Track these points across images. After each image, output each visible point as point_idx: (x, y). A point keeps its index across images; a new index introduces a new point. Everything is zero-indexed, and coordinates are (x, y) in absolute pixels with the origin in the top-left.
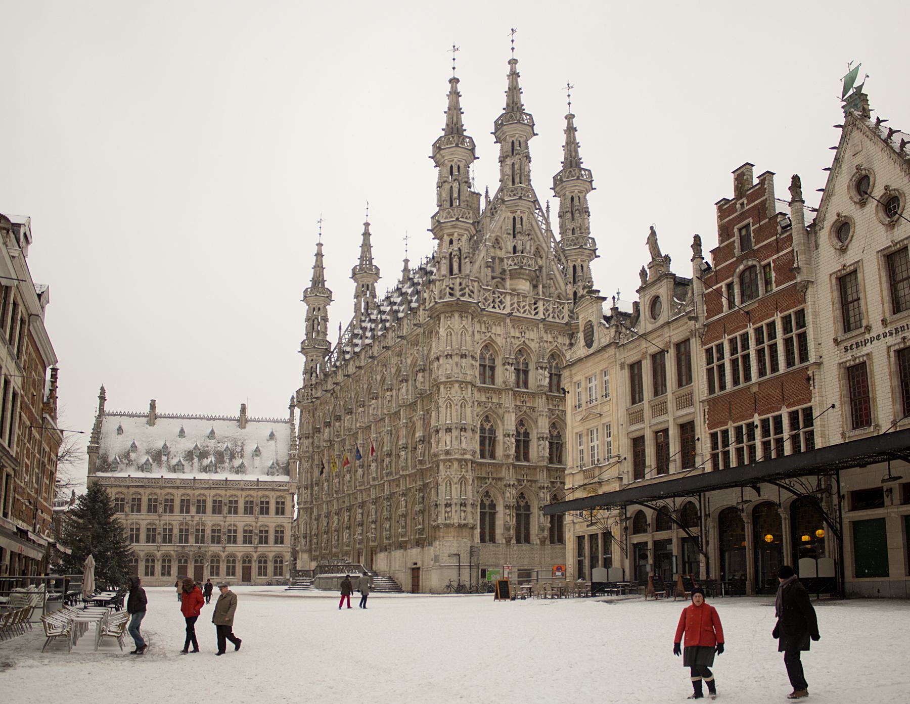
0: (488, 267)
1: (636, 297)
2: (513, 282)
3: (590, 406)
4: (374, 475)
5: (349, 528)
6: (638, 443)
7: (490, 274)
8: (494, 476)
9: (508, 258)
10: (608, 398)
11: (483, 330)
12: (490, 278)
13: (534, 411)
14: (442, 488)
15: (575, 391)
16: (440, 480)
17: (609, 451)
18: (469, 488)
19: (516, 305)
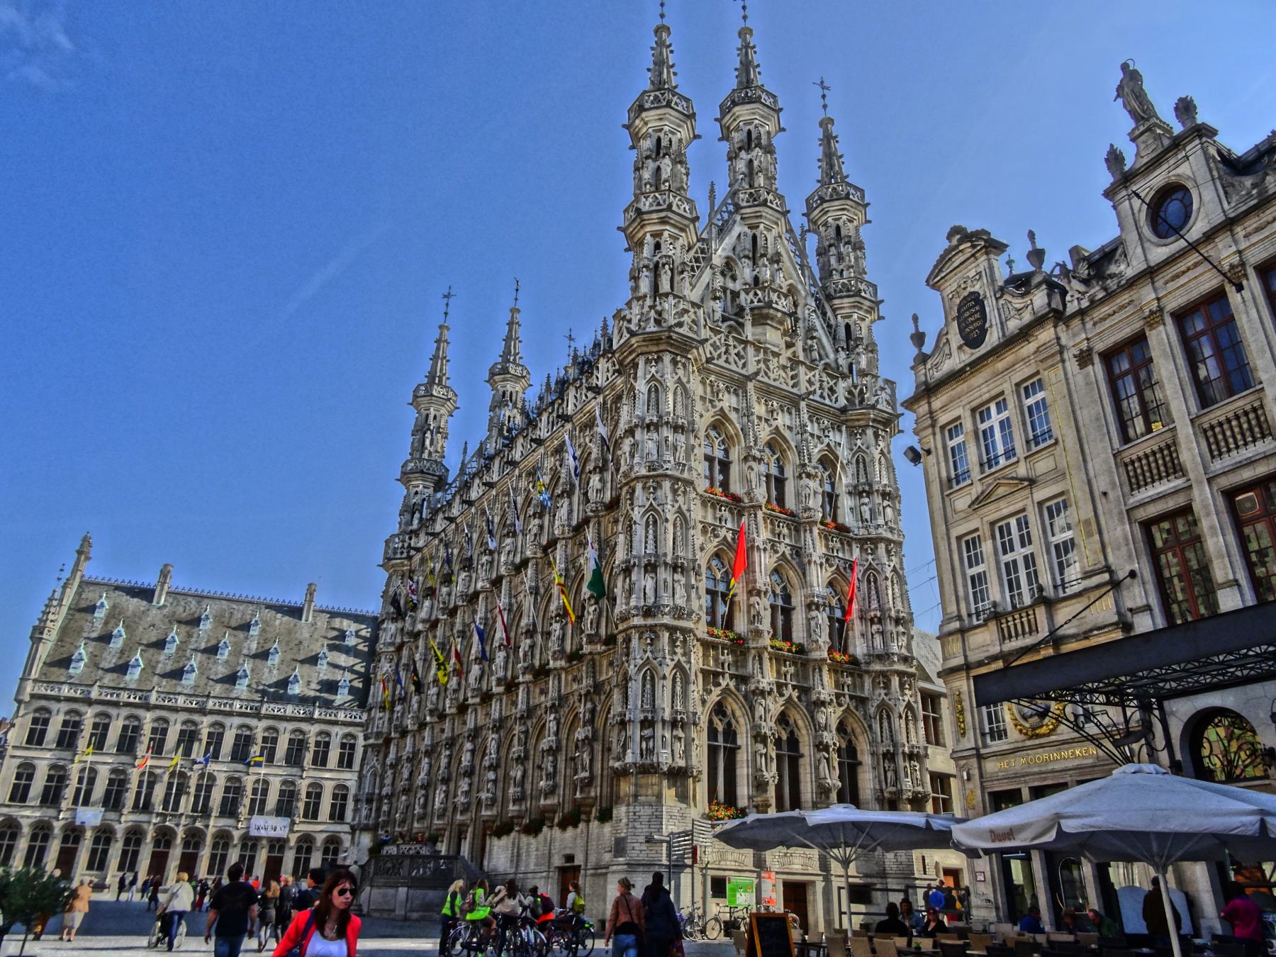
2: (759, 330)
5: (446, 781)
14: (635, 687)
15: (945, 447)
16: (632, 670)
19: (762, 365)
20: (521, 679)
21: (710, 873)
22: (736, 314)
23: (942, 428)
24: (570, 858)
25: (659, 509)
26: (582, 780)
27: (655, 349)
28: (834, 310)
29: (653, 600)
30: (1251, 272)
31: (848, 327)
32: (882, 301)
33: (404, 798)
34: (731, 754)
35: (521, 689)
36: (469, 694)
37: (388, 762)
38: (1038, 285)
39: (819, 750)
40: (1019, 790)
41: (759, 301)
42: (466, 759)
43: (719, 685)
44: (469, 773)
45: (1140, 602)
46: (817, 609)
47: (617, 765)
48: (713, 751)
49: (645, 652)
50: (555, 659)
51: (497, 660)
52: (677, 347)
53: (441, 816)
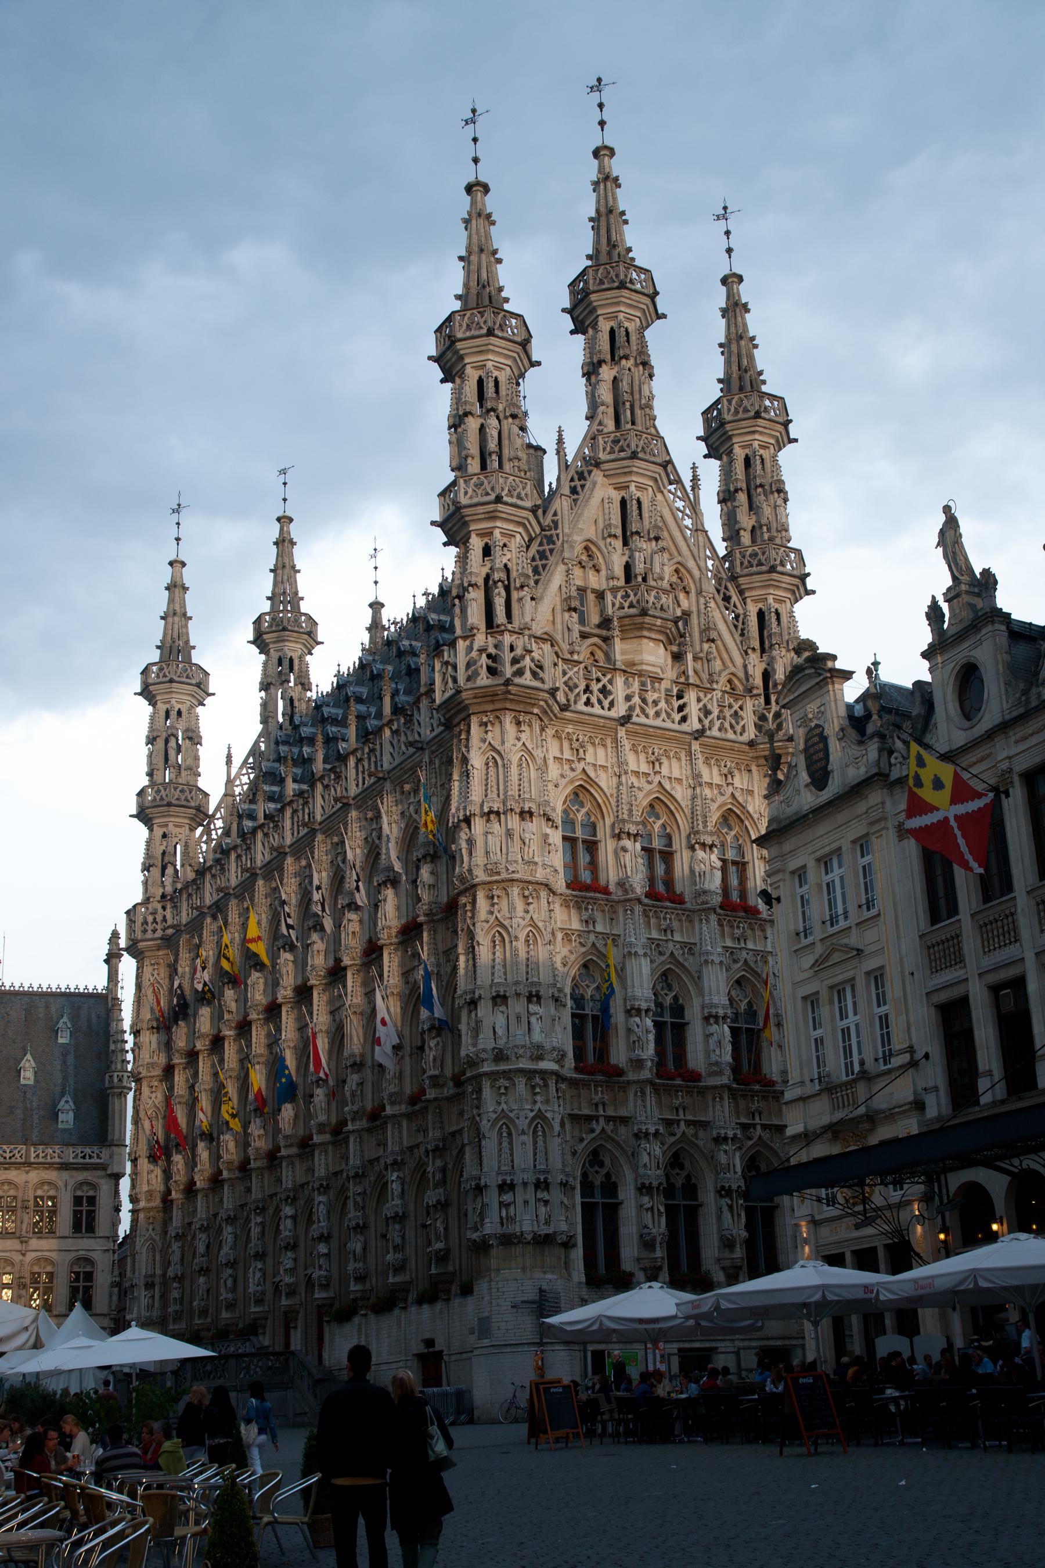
0: (571, 609)
1: (922, 671)
3: (831, 930)
4: (322, 1118)
6: (953, 1015)
7: (577, 628)
8: (610, 1112)
9: (614, 590)
10: (873, 912)
11: (567, 754)
12: (576, 634)
13: (691, 952)
14: (490, 1145)
15: (793, 895)
16: (485, 1126)
17: (886, 1038)
18: (555, 1144)
19: (636, 700)
20: (350, 1127)
21: (591, 1348)
22: (599, 626)
23: (793, 873)
24: (430, 1343)
25: (506, 923)
26: (438, 1252)
27: (491, 707)
28: (741, 592)
29: (505, 1040)
30: (1016, 779)
31: (761, 615)
32: (808, 575)
33: (202, 1280)
34: (612, 1211)
35: (352, 1139)
36: (282, 1144)
37: (172, 1232)
38: (871, 737)
39: (721, 1196)
40: (843, 1254)
41: (631, 606)
42: (287, 1227)
43: (592, 1131)
44: (292, 1247)
45: (930, 1084)
46: (717, 1023)
47: (475, 1236)
48: (588, 1209)
49: (499, 1103)
50: (393, 1103)
51: (316, 1099)
52: (519, 702)
53: (259, 1302)
